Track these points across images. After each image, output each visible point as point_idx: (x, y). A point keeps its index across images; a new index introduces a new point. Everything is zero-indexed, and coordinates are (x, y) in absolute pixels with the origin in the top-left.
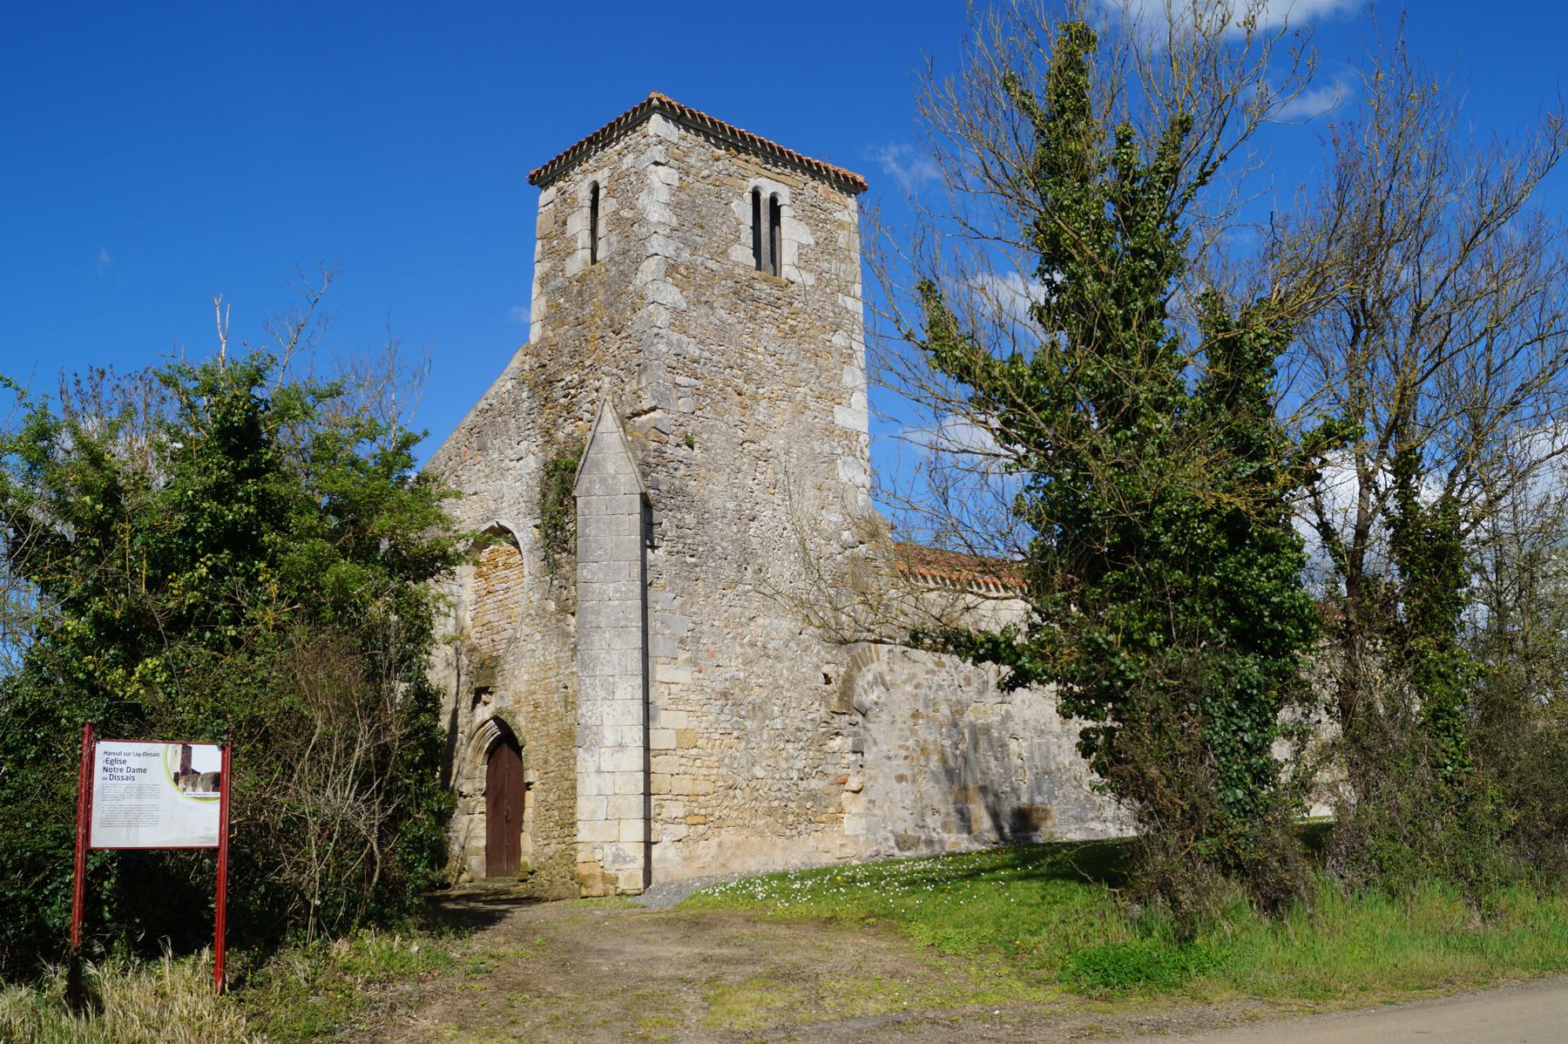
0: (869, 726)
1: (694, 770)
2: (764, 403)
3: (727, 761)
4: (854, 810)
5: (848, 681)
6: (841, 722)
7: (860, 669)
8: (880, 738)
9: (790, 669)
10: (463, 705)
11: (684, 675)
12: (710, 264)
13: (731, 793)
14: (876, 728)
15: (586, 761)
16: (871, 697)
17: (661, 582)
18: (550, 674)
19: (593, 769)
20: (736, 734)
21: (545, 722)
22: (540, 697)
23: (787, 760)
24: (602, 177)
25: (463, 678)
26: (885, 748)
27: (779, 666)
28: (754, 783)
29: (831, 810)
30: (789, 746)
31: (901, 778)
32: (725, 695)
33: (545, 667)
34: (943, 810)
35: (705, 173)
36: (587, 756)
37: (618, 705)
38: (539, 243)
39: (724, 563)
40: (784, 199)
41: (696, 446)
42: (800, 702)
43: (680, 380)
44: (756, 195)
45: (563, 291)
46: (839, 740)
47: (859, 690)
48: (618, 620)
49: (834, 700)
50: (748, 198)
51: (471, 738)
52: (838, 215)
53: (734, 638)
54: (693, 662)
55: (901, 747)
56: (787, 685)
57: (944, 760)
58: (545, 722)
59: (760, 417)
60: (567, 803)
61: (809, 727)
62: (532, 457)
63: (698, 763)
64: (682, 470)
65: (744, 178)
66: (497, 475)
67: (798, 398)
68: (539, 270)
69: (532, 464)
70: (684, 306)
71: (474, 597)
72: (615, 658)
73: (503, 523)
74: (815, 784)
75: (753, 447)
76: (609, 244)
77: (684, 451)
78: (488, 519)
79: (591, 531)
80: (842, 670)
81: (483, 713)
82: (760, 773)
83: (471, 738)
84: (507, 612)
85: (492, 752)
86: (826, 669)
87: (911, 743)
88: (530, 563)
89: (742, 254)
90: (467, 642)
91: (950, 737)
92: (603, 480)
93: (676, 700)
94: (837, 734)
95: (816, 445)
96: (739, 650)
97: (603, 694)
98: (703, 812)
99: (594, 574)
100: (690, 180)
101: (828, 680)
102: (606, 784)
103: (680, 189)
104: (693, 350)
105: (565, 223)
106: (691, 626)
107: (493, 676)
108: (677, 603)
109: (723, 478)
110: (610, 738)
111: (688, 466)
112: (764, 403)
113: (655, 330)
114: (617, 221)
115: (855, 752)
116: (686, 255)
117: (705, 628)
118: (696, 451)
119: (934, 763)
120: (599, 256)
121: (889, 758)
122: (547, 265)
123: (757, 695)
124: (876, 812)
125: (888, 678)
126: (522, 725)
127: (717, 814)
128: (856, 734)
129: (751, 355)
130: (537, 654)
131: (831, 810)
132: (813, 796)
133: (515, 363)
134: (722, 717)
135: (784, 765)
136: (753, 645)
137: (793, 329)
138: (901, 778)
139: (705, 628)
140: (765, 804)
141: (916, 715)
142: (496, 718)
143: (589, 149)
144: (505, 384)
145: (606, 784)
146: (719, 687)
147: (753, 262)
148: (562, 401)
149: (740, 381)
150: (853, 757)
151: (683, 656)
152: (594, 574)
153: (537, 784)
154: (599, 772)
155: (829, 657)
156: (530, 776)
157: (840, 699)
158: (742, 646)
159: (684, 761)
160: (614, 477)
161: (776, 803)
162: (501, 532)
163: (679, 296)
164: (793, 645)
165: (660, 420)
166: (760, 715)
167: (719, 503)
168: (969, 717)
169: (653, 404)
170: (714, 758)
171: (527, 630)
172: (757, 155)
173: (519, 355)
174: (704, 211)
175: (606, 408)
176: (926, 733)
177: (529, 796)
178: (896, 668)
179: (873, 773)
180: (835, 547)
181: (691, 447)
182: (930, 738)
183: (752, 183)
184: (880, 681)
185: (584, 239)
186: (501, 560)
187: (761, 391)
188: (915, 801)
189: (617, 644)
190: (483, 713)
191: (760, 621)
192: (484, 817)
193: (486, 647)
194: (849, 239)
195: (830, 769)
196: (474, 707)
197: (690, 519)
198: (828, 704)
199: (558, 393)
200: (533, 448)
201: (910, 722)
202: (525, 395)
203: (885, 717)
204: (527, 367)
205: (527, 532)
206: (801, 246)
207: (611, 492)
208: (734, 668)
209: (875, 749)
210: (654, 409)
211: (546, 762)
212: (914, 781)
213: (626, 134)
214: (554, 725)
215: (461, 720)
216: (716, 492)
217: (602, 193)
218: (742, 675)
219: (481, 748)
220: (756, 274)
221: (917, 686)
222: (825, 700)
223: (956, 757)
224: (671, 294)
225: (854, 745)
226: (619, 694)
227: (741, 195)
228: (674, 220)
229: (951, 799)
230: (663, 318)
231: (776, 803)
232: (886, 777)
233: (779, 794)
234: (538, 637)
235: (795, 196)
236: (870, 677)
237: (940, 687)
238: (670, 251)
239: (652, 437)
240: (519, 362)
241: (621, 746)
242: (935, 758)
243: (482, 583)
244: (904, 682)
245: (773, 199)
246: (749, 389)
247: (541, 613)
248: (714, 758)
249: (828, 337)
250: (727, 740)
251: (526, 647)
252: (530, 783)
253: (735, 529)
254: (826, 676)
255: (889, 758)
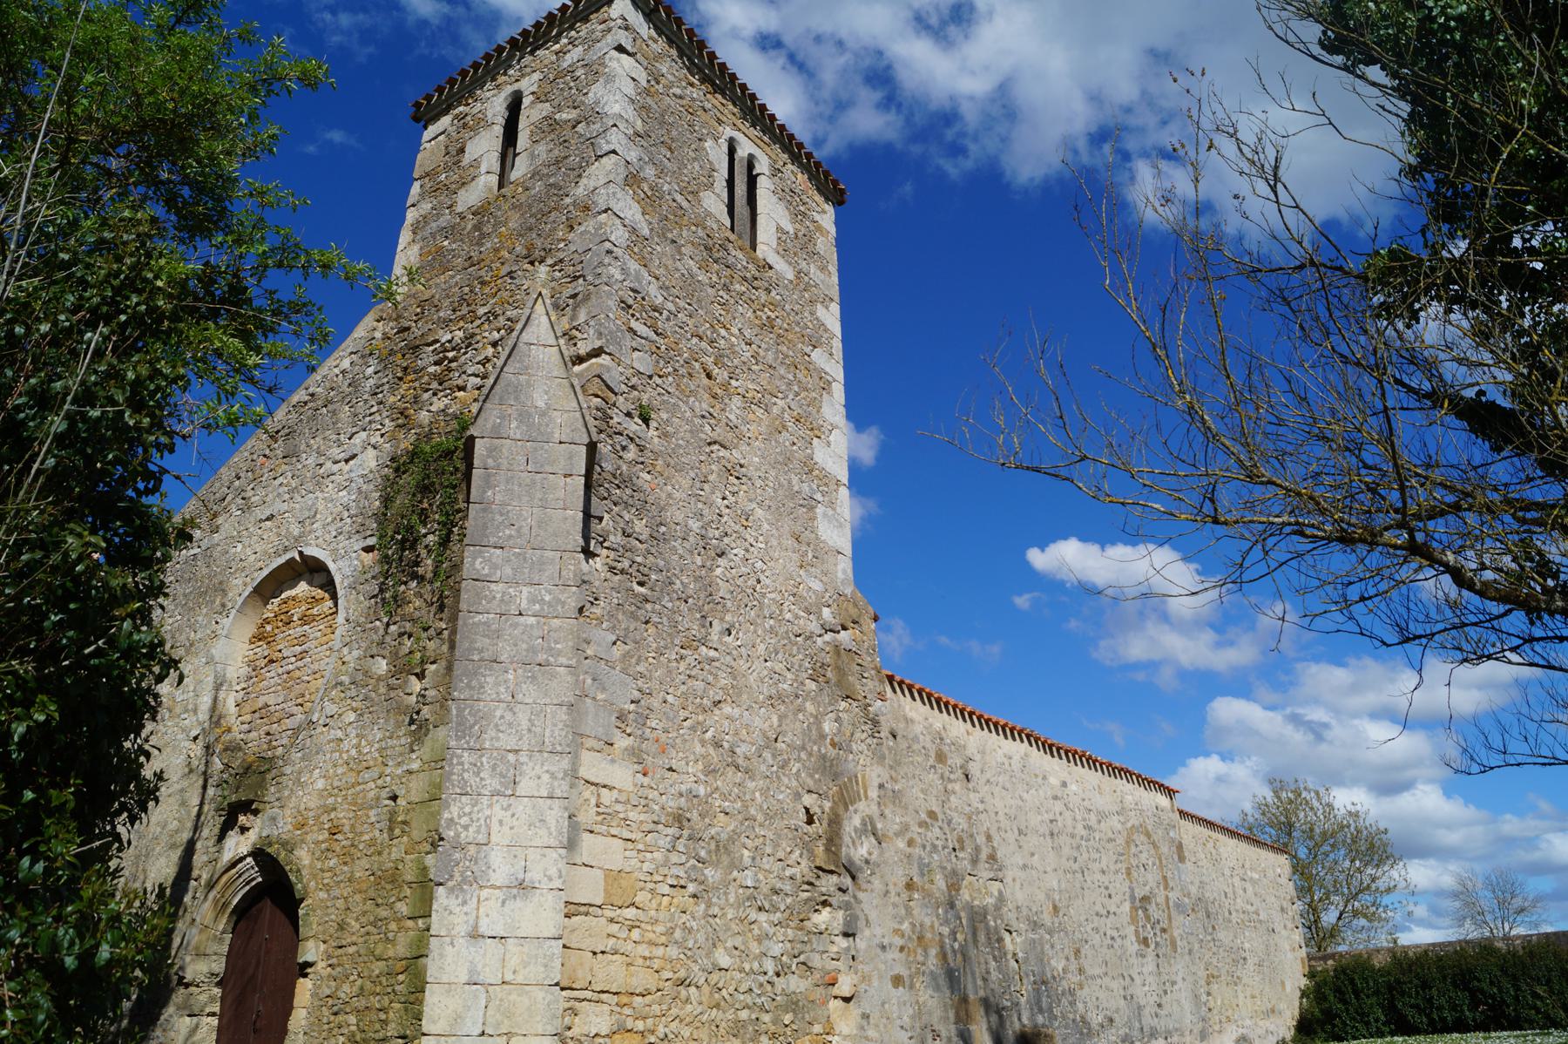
0: (861, 895)
1: (629, 946)
2: (737, 401)
3: (678, 934)
4: (846, 1031)
5: (835, 822)
6: (828, 883)
7: (847, 809)
8: (873, 915)
9: (765, 792)
10: (206, 832)
11: (622, 775)
12: (679, 198)
13: (683, 993)
14: (869, 902)
15: (448, 911)
16: (861, 850)
17: (597, 611)
18: (367, 775)
19: (462, 929)
20: (691, 888)
21: (347, 857)
22: (343, 815)
23: (759, 940)
24: (528, 85)
25: (211, 791)
26: (878, 931)
27: (751, 785)
28: (714, 977)
29: (817, 1028)
30: (763, 917)
31: (897, 981)
32: (679, 819)
33: (358, 765)
34: (944, 1034)
35: (678, 91)
36: (453, 903)
37: (522, 807)
38: (417, 185)
39: (683, 606)
40: (762, 166)
41: (653, 424)
42: (776, 845)
43: (633, 324)
44: (732, 151)
45: (449, 232)
46: (826, 912)
47: (847, 839)
48: (532, 650)
49: (820, 849)
50: (725, 148)
51: (210, 886)
52: (817, 217)
53: (693, 728)
54: (636, 755)
55: (896, 931)
56: (760, 818)
57: (943, 956)
58: (347, 857)
59: (732, 417)
60: (375, 1002)
61: (788, 888)
62: (371, 453)
63: (635, 934)
64: (631, 454)
65: (720, 122)
66: (310, 486)
67: (775, 410)
68: (411, 215)
69: (370, 460)
70: (646, 232)
71: (245, 670)
72: (523, 718)
73: (310, 551)
74: (796, 983)
75: (723, 453)
76: (533, 156)
77: (634, 426)
78: (286, 549)
79: (496, 495)
80: (827, 805)
81: (237, 845)
82: (725, 961)
83: (210, 886)
84: (298, 689)
85: (243, 914)
86: (808, 800)
87: (906, 926)
88: (352, 604)
89: (714, 203)
90: (227, 737)
91: (946, 922)
92: (524, 417)
93: (605, 815)
94: (825, 903)
95: (795, 480)
96: (698, 749)
97: (493, 783)
98: (640, 1025)
99: (495, 567)
100: (660, 88)
101: (810, 821)
102: (488, 961)
103: (647, 92)
104: (654, 293)
105: (462, 150)
106: (636, 695)
107: (262, 785)
108: (617, 651)
109: (686, 483)
110: (501, 868)
111: (641, 449)
112: (737, 401)
113: (608, 245)
114: (550, 125)
115: (846, 935)
116: (649, 172)
117: (655, 703)
118: (652, 432)
119: (933, 962)
120: (515, 175)
121: (883, 948)
122: (426, 206)
123: (722, 827)
124: (871, 1033)
125: (879, 826)
126: (304, 862)
127: (661, 1031)
128: (847, 906)
129: (723, 332)
130: (346, 745)
131: (817, 1028)
132: (793, 1004)
133: (360, 332)
134: (674, 858)
135: (755, 948)
136: (718, 745)
137: (770, 325)
138: (897, 981)
139: (655, 703)
140: (730, 1015)
141: (910, 886)
142: (258, 854)
143: (511, 57)
144: (340, 362)
145: (488, 961)
146: (672, 804)
147: (728, 223)
148: (432, 369)
149: (710, 360)
150: (843, 943)
151: (622, 742)
152: (495, 567)
153: (321, 965)
154: (475, 935)
155: (810, 783)
156: (310, 951)
157: (827, 850)
158: (703, 743)
159: (614, 928)
160: (543, 414)
161: (744, 1014)
162: (313, 570)
163: (639, 217)
164: (767, 755)
165: (608, 369)
166: (725, 860)
167: (679, 517)
168: (965, 895)
169: (598, 344)
170: (660, 929)
171: (331, 708)
172: (735, 105)
173: (369, 321)
174: (674, 133)
175: (539, 307)
176: (925, 917)
177: (304, 988)
178: (887, 812)
179: (866, 968)
180: (814, 627)
181: (646, 420)
182: (927, 921)
183: (729, 132)
184: (869, 828)
185: (491, 161)
186: (297, 613)
187: (733, 382)
188: (912, 1017)
189: (529, 693)
190: (237, 845)
191: (727, 709)
192: (215, 1021)
193: (255, 743)
194: (826, 244)
195: (816, 961)
196: (221, 837)
197: (639, 526)
198: (811, 853)
199: (428, 356)
200: (376, 438)
201: (905, 896)
202: (370, 370)
203: (877, 883)
204: (378, 335)
205: (348, 562)
206: (779, 229)
207: (537, 438)
208: (690, 777)
209: (867, 932)
210: (597, 353)
211: (342, 926)
212: (912, 987)
213: (572, 28)
214: (365, 863)
215: (199, 859)
216: (674, 495)
217: (526, 101)
218: (702, 791)
219: (225, 905)
220: (733, 237)
221: (910, 843)
222: (807, 847)
223: (954, 951)
224: (630, 209)
225: (847, 923)
226: (525, 786)
227: (716, 139)
228: (639, 122)
229: (951, 1014)
230: (619, 235)
231: (744, 1014)
232: (881, 977)
233: (748, 999)
234: (352, 717)
235: (776, 172)
236: (857, 821)
237: (934, 846)
238: (633, 155)
239: (594, 388)
240: (369, 328)
241: (522, 887)
242: (933, 952)
243: (262, 649)
244: (897, 835)
245: (750, 163)
246: (721, 374)
247: (362, 678)
248: (660, 929)
249: (808, 349)
250: (682, 899)
251: (323, 735)
252: (310, 965)
253: (699, 561)
254: (807, 810)
255: (883, 948)
